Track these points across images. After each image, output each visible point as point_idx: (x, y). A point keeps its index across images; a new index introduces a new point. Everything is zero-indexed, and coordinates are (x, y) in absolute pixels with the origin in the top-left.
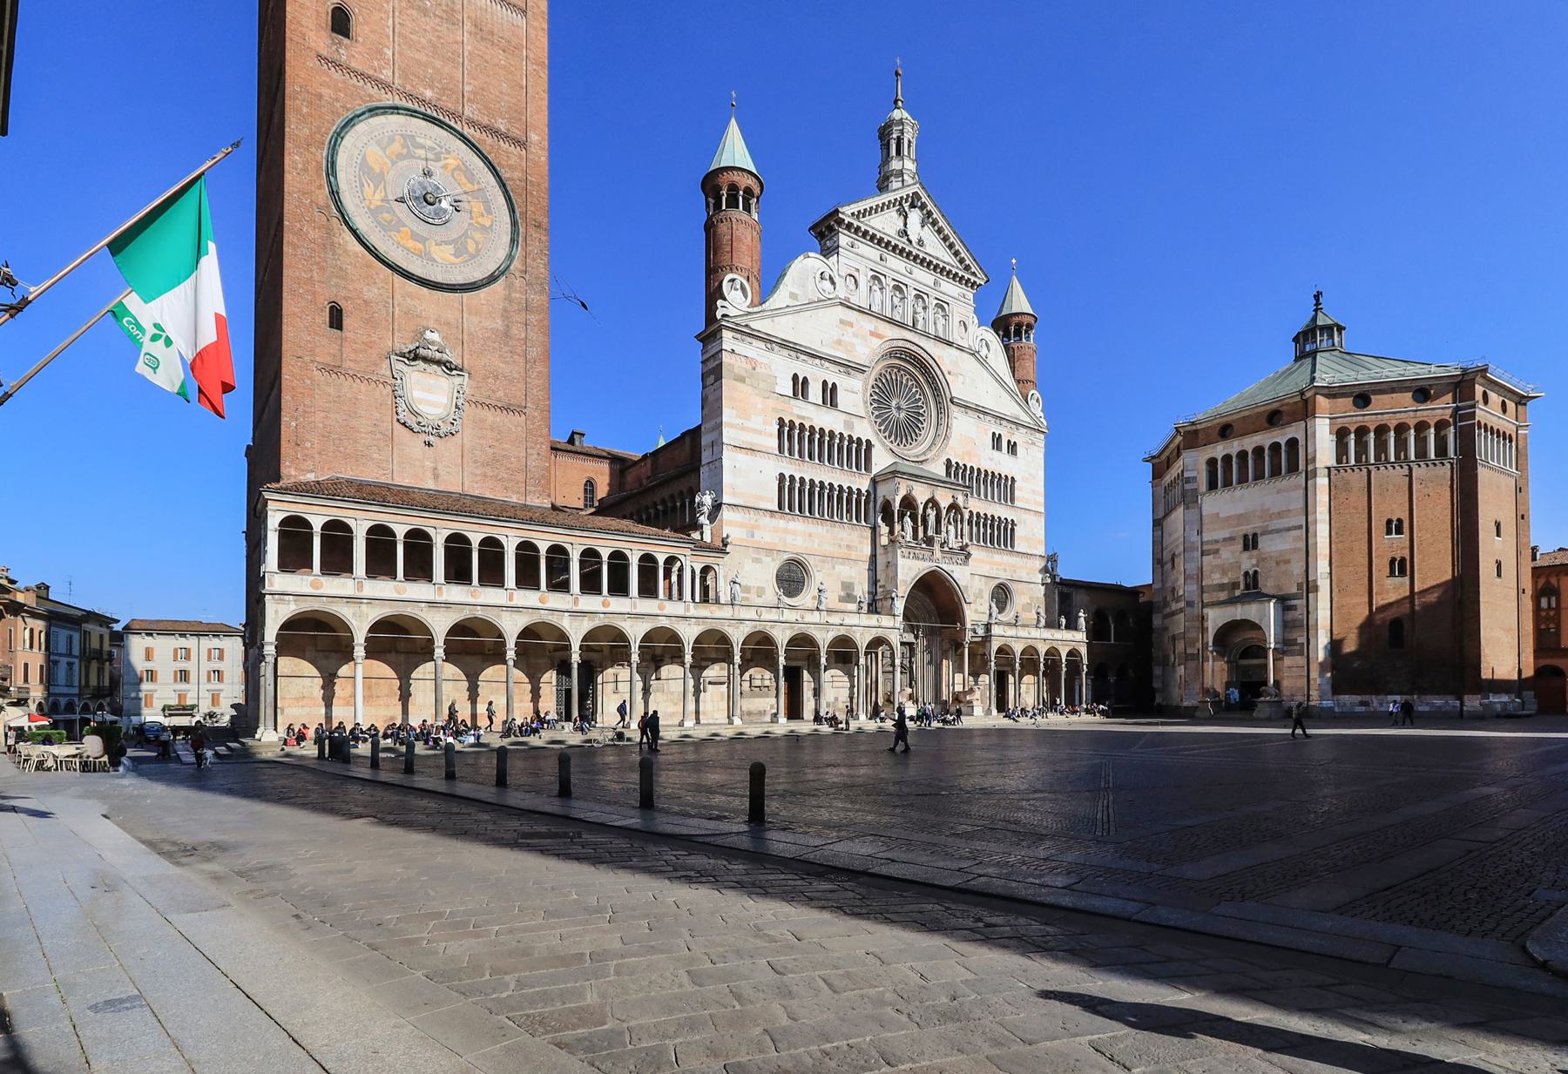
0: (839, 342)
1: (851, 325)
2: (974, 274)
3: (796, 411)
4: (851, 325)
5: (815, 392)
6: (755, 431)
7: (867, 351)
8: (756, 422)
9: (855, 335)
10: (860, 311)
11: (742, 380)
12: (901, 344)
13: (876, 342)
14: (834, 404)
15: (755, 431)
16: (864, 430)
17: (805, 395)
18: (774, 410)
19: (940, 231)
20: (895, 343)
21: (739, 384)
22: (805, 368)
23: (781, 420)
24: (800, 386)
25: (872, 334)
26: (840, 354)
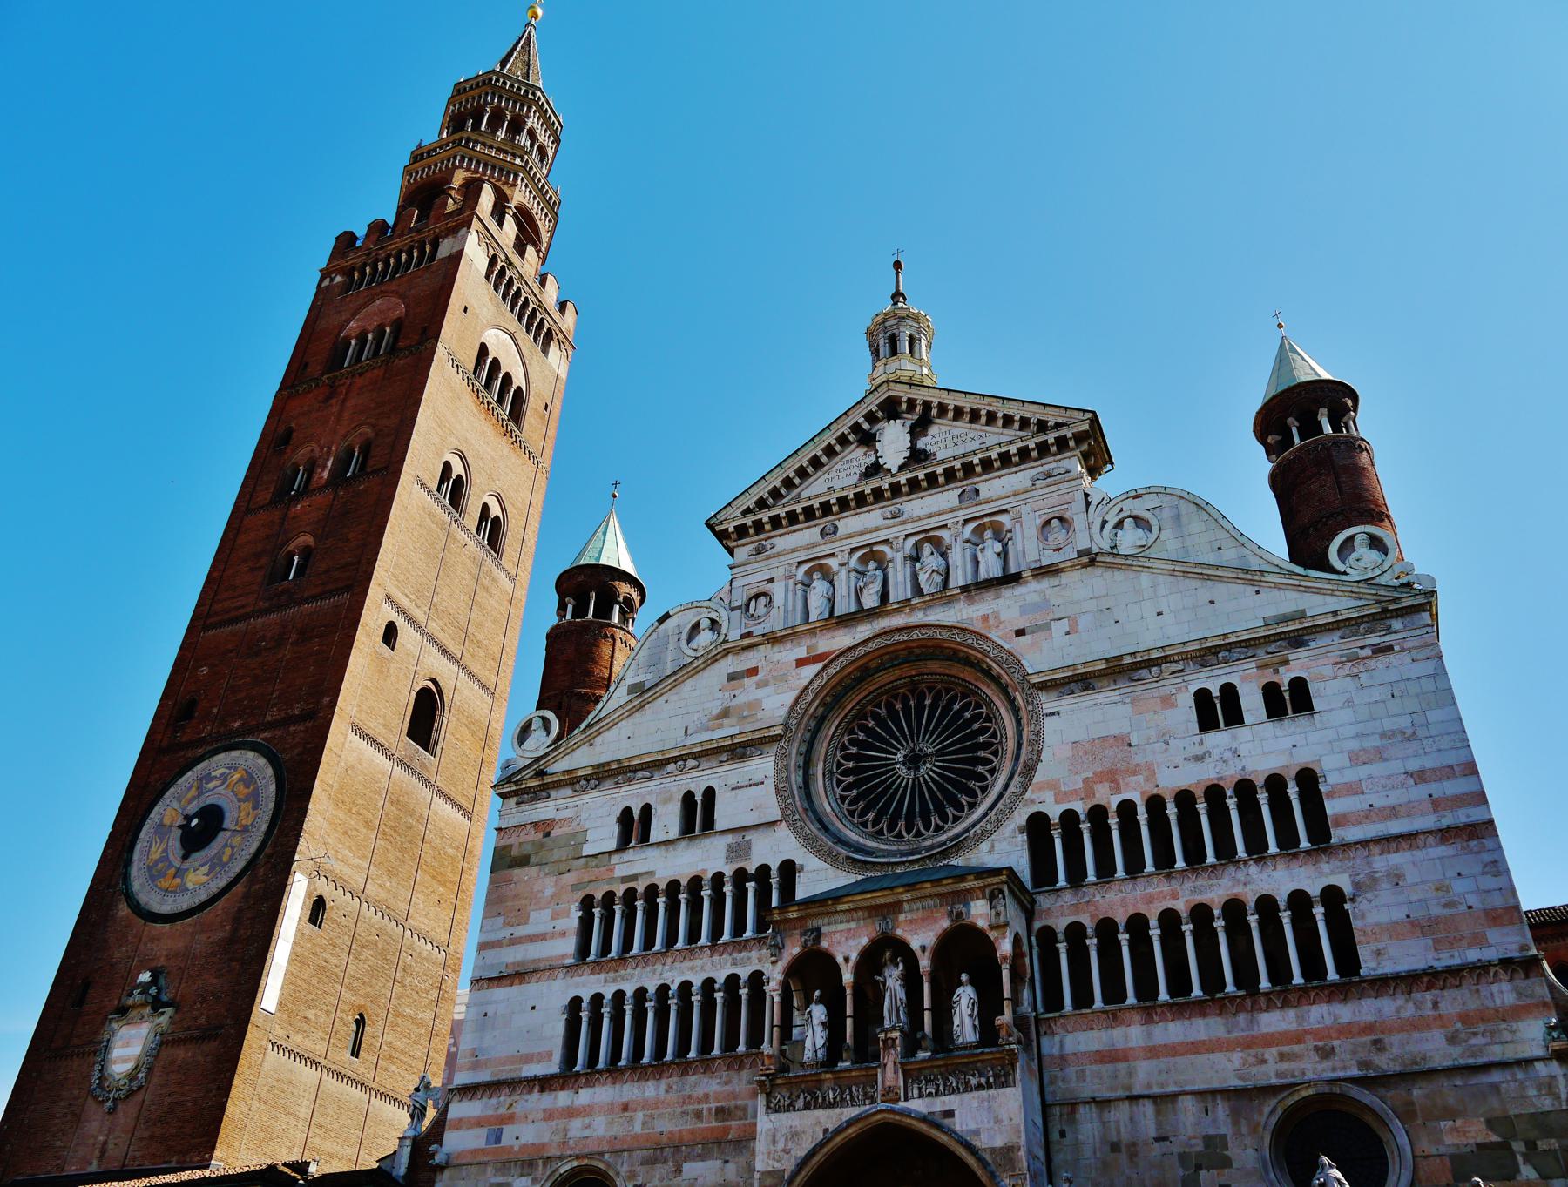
0: (725, 714)
1: (753, 671)
2: (1058, 425)
3: (621, 871)
4: (753, 671)
5: (666, 822)
6: (533, 939)
7: (789, 698)
8: (539, 920)
9: (762, 685)
10: (774, 639)
11: (523, 861)
12: (872, 645)
13: (810, 671)
14: (709, 823)
15: (533, 939)
16: (772, 849)
17: (645, 838)
18: (575, 888)
19: (958, 413)
20: (862, 650)
21: (516, 871)
22: (633, 796)
23: (587, 903)
24: (634, 828)
25: (801, 663)
26: (728, 730)
